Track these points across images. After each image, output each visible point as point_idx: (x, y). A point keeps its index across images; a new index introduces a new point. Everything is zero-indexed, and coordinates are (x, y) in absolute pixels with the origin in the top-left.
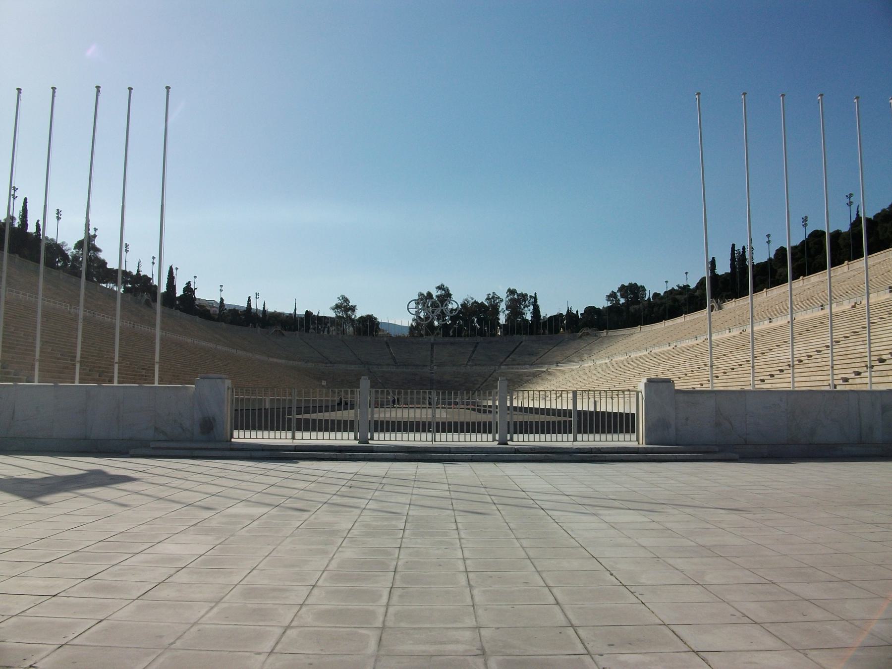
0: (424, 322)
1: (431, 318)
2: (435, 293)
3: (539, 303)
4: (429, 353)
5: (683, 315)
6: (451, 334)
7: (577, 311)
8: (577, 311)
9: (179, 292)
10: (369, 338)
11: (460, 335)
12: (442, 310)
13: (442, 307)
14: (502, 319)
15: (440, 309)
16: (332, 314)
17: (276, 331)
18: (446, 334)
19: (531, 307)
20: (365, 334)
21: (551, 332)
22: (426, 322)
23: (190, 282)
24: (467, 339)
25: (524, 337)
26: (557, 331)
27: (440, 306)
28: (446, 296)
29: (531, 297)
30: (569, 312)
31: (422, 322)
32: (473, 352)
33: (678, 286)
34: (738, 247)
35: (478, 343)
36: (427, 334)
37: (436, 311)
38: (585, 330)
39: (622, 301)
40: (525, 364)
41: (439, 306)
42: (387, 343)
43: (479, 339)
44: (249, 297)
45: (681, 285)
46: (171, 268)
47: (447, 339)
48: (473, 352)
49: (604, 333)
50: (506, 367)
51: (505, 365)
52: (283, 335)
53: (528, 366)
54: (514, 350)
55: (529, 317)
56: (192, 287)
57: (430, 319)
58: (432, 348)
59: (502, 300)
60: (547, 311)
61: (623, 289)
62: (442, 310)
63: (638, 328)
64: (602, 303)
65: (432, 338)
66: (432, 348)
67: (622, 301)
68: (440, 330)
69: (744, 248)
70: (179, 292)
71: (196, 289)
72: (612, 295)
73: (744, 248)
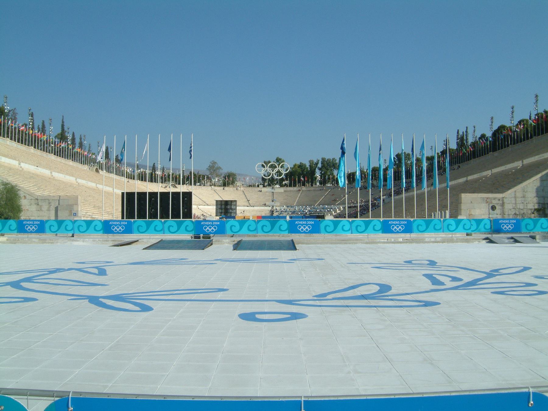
1: (272, 174)
11: (290, 186)
13: (279, 167)
14: (318, 175)
15: (278, 168)
16: (208, 173)
18: (282, 186)
22: (268, 178)
24: (295, 189)
31: (265, 178)
34: (461, 133)
36: (269, 185)
41: (276, 167)
42: (243, 191)
44: (154, 163)
57: (271, 175)
62: (279, 169)
69: (463, 132)
73: (463, 132)
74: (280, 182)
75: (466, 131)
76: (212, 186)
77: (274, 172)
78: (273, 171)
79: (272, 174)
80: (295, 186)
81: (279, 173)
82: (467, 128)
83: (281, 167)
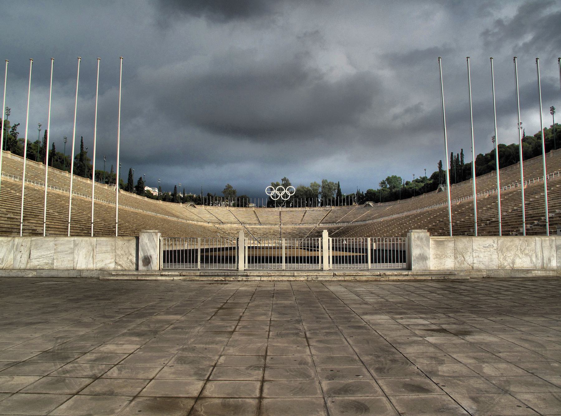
0: (275, 199)
2: (281, 182)
3: (341, 187)
4: (278, 217)
5: (424, 194)
6: (291, 206)
7: (363, 192)
8: (363, 192)
9: (135, 183)
10: (244, 209)
11: (296, 207)
12: (285, 192)
15: (285, 191)
17: (191, 205)
18: (288, 206)
19: (336, 191)
20: (242, 206)
21: (348, 204)
22: (277, 199)
23: (141, 178)
24: (300, 209)
25: (333, 208)
26: (351, 204)
27: (284, 190)
28: (286, 184)
29: (336, 184)
30: (358, 193)
31: (274, 199)
32: (304, 216)
33: (420, 177)
34: (455, 154)
35: (306, 211)
37: (282, 193)
38: (367, 203)
39: (388, 186)
40: (333, 223)
43: (307, 209)
45: (422, 177)
46: (130, 170)
47: (288, 209)
48: (304, 216)
49: (379, 204)
50: (323, 224)
51: (322, 223)
52: (195, 207)
53: (335, 224)
54: (327, 215)
55: (335, 196)
56: (143, 180)
57: (279, 197)
58: (280, 214)
59: (319, 186)
60: (345, 193)
61: (388, 179)
62: (285, 192)
63: (398, 201)
64: (376, 187)
65: (280, 209)
66: (280, 214)
67: (388, 186)
68: (284, 203)
69: (458, 155)
70: (135, 183)
71: (145, 181)
72: (383, 183)
74: (288, 204)
75: (462, 153)
76: (227, 207)
77: (282, 194)
78: (280, 194)
79: (279, 196)
80: (299, 207)
81: (286, 196)
82: (462, 150)
83: (288, 190)
